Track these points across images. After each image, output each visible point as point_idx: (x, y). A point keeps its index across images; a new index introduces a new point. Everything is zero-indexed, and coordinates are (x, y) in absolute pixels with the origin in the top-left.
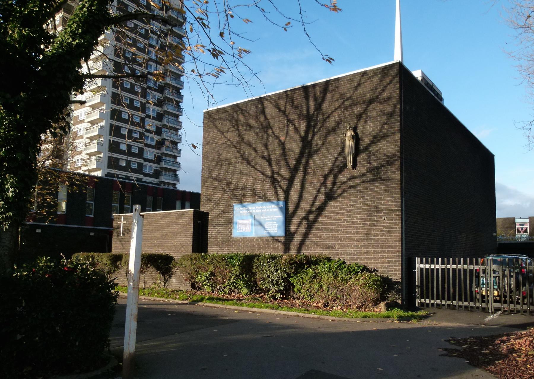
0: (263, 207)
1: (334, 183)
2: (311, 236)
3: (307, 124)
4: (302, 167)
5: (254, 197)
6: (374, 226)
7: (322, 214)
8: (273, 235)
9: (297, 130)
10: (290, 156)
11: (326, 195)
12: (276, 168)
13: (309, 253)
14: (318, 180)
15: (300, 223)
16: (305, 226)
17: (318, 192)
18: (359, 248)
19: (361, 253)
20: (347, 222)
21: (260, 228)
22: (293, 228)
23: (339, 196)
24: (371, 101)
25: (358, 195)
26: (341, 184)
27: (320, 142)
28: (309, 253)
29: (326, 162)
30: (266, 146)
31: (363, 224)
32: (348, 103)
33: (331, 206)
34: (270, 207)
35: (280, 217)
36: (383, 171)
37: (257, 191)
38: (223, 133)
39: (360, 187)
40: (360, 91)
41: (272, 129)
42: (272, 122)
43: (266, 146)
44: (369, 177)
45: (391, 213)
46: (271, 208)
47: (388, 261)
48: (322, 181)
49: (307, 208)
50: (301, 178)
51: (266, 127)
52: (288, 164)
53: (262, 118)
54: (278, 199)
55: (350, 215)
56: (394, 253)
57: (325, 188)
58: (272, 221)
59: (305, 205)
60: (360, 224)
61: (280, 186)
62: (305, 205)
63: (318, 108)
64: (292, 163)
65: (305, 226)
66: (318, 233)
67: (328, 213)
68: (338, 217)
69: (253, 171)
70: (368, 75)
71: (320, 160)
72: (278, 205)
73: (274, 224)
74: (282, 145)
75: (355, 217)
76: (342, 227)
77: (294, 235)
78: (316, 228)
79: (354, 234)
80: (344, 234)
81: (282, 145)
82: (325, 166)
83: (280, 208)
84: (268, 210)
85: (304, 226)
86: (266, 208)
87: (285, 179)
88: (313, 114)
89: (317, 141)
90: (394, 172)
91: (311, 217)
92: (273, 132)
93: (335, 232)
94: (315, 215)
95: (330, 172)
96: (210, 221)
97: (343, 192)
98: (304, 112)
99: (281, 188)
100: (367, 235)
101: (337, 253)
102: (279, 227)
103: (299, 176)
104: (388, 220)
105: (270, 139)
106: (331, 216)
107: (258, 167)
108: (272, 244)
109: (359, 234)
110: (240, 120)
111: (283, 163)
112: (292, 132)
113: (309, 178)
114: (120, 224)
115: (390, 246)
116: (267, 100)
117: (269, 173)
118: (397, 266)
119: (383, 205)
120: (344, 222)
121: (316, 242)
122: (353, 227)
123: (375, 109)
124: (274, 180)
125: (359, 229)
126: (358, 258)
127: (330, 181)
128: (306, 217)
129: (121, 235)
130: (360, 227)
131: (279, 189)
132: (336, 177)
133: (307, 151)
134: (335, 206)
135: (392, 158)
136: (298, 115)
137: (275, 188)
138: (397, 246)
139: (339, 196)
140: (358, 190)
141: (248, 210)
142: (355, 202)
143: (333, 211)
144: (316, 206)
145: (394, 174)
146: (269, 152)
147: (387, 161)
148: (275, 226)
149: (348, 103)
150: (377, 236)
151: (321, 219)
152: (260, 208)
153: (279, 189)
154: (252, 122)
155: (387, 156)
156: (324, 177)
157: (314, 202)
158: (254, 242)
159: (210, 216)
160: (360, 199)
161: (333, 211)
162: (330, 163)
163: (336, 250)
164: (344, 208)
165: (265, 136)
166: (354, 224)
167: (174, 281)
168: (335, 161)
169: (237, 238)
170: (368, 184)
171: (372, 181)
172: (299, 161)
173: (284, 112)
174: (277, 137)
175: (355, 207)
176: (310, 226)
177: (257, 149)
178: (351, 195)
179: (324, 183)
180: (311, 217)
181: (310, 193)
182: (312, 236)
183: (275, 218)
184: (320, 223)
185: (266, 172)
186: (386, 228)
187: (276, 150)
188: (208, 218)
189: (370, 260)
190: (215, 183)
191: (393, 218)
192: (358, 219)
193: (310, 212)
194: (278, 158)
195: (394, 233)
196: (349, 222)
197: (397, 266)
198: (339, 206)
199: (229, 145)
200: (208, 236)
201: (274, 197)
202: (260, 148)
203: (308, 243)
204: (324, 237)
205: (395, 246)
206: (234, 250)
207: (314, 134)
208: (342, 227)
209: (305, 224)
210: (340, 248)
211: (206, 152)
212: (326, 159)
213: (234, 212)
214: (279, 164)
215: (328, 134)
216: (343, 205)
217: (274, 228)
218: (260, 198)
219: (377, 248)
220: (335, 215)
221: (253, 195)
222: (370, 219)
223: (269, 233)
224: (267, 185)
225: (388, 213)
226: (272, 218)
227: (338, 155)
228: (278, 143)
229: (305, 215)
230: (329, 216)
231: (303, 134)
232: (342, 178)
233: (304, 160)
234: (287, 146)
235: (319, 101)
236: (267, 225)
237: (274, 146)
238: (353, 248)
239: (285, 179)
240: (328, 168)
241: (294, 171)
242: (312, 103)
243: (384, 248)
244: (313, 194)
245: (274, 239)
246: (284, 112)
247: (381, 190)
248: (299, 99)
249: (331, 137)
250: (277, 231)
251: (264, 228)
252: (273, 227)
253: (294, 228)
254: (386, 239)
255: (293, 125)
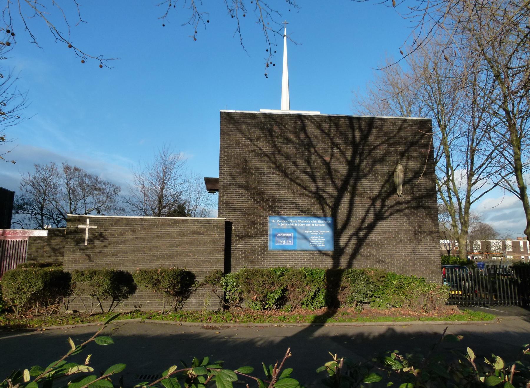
0: (307, 222)
1: (383, 206)
2: (362, 251)
3: (353, 150)
4: (349, 188)
5: (295, 211)
6: (419, 244)
7: (372, 231)
8: (321, 249)
9: (343, 154)
10: (336, 176)
11: (374, 215)
12: (320, 184)
13: (360, 266)
14: (368, 202)
15: (350, 239)
16: (354, 242)
17: (367, 212)
18: (407, 262)
19: (409, 266)
20: (395, 240)
21: (304, 241)
22: (342, 243)
23: (387, 218)
24: (412, 144)
25: (404, 218)
26: (389, 208)
27: (367, 169)
28: (360, 266)
29: (373, 187)
30: (308, 162)
31: (410, 242)
32: (391, 141)
33: (379, 225)
34: (316, 222)
35: (328, 232)
36: (424, 200)
37: (298, 205)
38: (251, 140)
39: (406, 211)
40: (402, 133)
41: (314, 148)
42: (315, 142)
43: (308, 162)
44: (414, 204)
45: (432, 234)
46: (317, 223)
47: (432, 272)
48: (370, 203)
49: (356, 225)
50: (348, 198)
51: (309, 144)
52: (335, 184)
53: (302, 136)
54: (325, 215)
55: (398, 234)
56: (436, 266)
57: (374, 210)
58: (318, 235)
59: (355, 223)
60: (407, 242)
61: (326, 203)
62: (355, 223)
63: (365, 138)
64: (339, 183)
65: (354, 242)
66: (369, 248)
67: (377, 232)
68: (387, 235)
69: (293, 185)
70: (408, 123)
71: (367, 184)
72: (326, 220)
73: (320, 238)
74: (327, 165)
75: (402, 236)
76: (391, 244)
77: (344, 250)
78: (366, 244)
79: (403, 250)
80: (393, 250)
81: (327, 165)
82: (372, 191)
83: (328, 224)
84: (313, 225)
85: (354, 241)
86: (311, 223)
87: (331, 196)
88: (359, 143)
89: (364, 167)
90: (432, 203)
91: (362, 234)
92: (316, 151)
93: (385, 248)
94: (364, 233)
95: (378, 197)
96: (233, 232)
97: (391, 214)
98: (350, 139)
99: (328, 205)
100: (414, 252)
101: (388, 266)
102: (327, 242)
103: (347, 196)
104: (430, 240)
105: (313, 157)
106: (380, 234)
107: (298, 181)
108: (318, 258)
109: (407, 250)
110: (275, 131)
111: (328, 181)
112: (338, 155)
113: (357, 199)
114: (84, 230)
115: (433, 260)
116: (308, 119)
117: (313, 187)
118: (439, 276)
119: (425, 228)
120: (393, 240)
121: (367, 256)
122: (401, 244)
123: (416, 151)
124: (319, 196)
125: (406, 246)
126: (407, 270)
127: (378, 204)
128: (356, 234)
129: (86, 243)
130: (407, 244)
131: (324, 205)
132: (383, 201)
133: (354, 174)
134: (383, 225)
135: (431, 191)
136: (343, 141)
137: (321, 204)
138: (438, 260)
139: (387, 218)
140: (404, 214)
141: (289, 223)
142: (402, 224)
143: (381, 230)
144: (365, 225)
145: (433, 205)
146: (312, 168)
147: (427, 193)
148: (323, 241)
149: (391, 141)
150: (421, 252)
151: (371, 236)
152: (304, 222)
153: (324, 205)
154: (292, 137)
155: (426, 189)
156: (372, 200)
157: (364, 220)
158: (297, 255)
159: (233, 226)
160: (406, 222)
161: (381, 230)
162: (377, 189)
163: (386, 264)
164: (392, 228)
165: (307, 153)
166: (402, 242)
167: (194, 302)
168: (383, 186)
169: (273, 251)
170: (412, 210)
171: (416, 208)
172: (346, 182)
173: (328, 135)
174: (321, 157)
175: (402, 228)
176: (360, 242)
177: (298, 164)
178: (398, 218)
179: (373, 204)
180: (362, 234)
181: (359, 212)
182: (364, 250)
183: (322, 233)
184: (370, 240)
185: (309, 187)
186: (429, 246)
187: (321, 168)
188: (231, 228)
189: (417, 272)
190: (242, 191)
191: (434, 238)
192: (405, 238)
193: (360, 229)
194: (323, 176)
195: (435, 250)
196: (397, 240)
197: (439, 276)
198: (387, 225)
199: (258, 155)
200: (231, 249)
201: (320, 213)
202: (301, 163)
203: (358, 257)
204: (374, 252)
205: (437, 260)
206: (270, 265)
207: (361, 161)
208: (391, 244)
209: (354, 240)
210: (390, 262)
211: (226, 156)
212: (373, 185)
213: (269, 225)
214: (324, 180)
215: (375, 162)
216: (391, 226)
217: (321, 243)
218: (302, 213)
219: (422, 262)
220: (384, 234)
221: (293, 209)
222: (415, 238)
223: (316, 247)
224: (310, 201)
225: (430, 234)
226: (318, 233)
227: (385, 183)
228: (322, 162)
229: (354, 231)
230: (378, 234)
231: (349, 158)
232: (390, 202)
233: (351, 182)
234: (333, 167)
235: (365, 133)
236: (313, 239)
237: (317, 163)
238: (401, 262)
239: (331, 196)
240: (376, 192)
241: (341, 191)
242: (357, 133)
243: (428, 262)
244: (361, 213)
245: (321, 252)
246: (328, 135)
247: (423, 216)
248: (343, 126)
249: (378, 167)
250: (324, 246)
251: (309, 241)
252: (320, 241)
253: (342, 244)
254: (429, 254)
255: (339, 148)
